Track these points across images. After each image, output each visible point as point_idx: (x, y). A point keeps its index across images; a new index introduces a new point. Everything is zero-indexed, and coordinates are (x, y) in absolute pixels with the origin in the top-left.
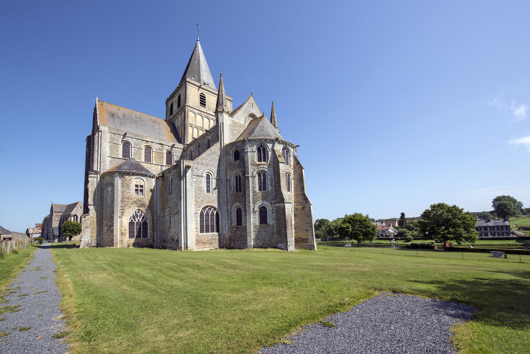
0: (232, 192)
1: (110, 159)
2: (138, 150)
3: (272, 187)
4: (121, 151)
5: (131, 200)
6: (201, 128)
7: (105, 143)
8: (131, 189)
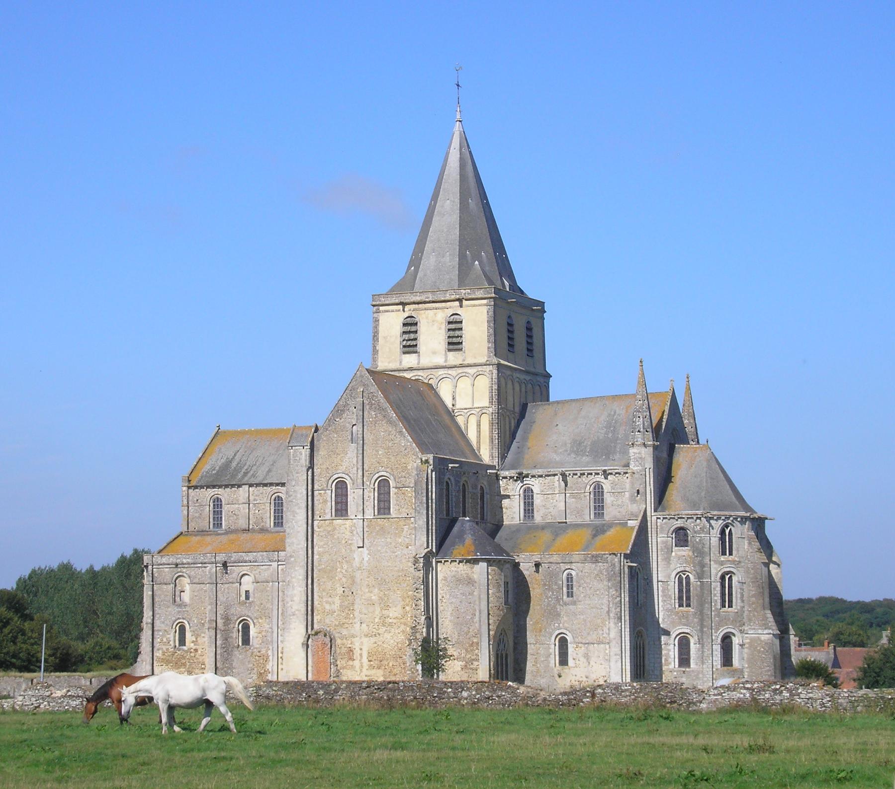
0: (671, 605)
3: (743, 601)
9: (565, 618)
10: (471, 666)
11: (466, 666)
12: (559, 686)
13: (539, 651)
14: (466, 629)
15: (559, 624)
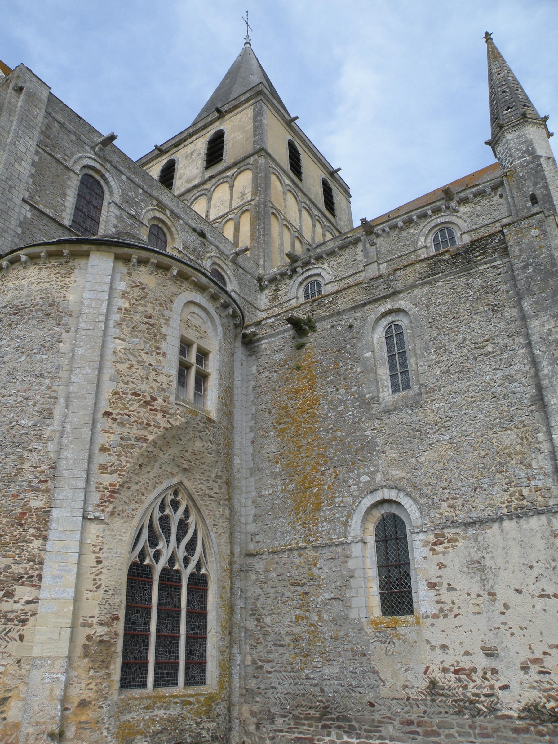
1: (29, 215)
2: (130, 221)
4: (71, 200)
5: (160, 415)
6: (298, 232)
7: (27, 139)
8: (165, 354)
9: (391, 454)
12: (384, 691)
13: (315, 571)
15: (371, 474)
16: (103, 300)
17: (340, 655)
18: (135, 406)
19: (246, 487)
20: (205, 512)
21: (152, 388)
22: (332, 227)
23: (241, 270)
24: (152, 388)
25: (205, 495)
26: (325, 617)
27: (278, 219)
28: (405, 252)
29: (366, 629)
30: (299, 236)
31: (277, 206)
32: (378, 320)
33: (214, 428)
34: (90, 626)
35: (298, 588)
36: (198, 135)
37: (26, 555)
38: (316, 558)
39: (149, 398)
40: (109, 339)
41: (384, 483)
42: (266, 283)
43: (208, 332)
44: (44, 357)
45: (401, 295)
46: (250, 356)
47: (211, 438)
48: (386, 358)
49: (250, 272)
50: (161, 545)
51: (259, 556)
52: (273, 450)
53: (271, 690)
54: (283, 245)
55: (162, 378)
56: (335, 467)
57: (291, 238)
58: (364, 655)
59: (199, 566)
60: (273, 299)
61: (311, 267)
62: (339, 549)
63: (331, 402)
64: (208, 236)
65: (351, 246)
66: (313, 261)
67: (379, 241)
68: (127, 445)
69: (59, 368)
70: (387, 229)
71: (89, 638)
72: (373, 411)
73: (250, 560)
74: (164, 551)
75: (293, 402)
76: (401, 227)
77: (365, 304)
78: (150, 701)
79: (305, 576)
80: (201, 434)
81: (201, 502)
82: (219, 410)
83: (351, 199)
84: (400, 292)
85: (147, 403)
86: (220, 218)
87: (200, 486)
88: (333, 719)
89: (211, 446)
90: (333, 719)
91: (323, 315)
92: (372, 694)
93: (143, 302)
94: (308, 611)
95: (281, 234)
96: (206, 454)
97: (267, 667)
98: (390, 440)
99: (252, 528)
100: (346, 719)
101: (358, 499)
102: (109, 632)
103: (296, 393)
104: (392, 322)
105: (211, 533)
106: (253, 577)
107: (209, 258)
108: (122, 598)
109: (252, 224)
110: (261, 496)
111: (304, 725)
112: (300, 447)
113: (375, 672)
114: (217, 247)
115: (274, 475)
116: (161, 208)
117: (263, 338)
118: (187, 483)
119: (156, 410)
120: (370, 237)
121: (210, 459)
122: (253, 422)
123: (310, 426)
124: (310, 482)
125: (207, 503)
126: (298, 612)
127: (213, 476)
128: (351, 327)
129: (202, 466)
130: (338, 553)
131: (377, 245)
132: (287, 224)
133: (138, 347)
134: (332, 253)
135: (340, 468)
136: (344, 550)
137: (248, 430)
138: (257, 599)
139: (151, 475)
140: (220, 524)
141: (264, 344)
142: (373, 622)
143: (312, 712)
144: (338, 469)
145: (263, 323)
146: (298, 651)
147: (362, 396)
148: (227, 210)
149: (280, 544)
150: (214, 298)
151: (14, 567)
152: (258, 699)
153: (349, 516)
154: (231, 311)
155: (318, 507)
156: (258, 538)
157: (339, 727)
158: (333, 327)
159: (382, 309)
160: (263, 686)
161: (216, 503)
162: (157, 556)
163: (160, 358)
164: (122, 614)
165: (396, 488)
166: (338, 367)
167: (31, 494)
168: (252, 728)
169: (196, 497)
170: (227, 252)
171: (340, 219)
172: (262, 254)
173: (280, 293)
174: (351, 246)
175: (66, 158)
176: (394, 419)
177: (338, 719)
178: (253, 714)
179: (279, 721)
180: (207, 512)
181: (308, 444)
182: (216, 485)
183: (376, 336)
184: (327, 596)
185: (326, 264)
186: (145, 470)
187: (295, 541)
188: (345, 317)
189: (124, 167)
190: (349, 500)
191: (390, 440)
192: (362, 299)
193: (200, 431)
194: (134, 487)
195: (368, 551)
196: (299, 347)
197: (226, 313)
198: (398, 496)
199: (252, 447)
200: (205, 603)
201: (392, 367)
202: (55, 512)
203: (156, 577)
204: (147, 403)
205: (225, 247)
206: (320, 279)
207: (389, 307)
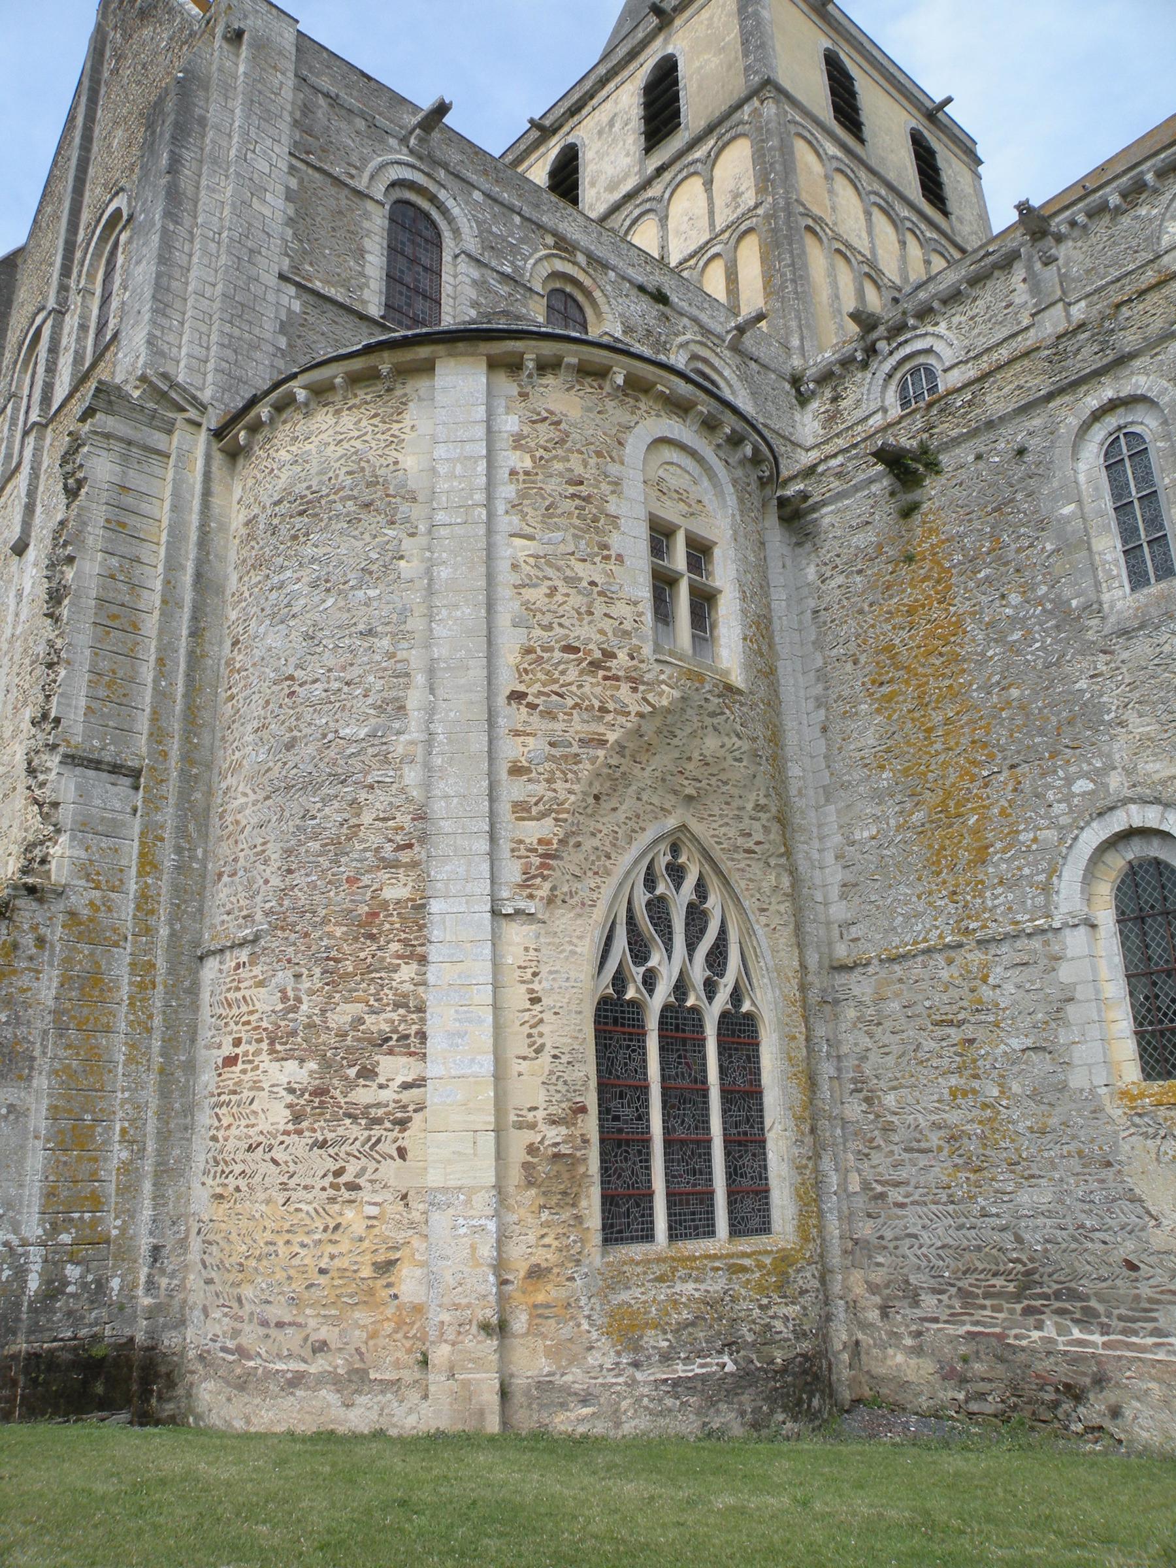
1: (297, 306)
2: (503, 290)
4: (375, 262)
5: (625, 688)
7: (269, 142)
8: (620, 558)
9: (1141, 726)
10: (364, 1095)
11: (320, 1092)
13: (986, 992)
14: (333, 814)
15: (1097, 776)
16: (475, 459)
17: (1054, 1166)
18: (572, 674)
19: (820, 826)
20: (740, 884)
21: (602, 632)
22: (944, 241)
23: (753, 365)
24: (602, 632)
25: (736, 848)
26: (1016, 1088)
27: (820, 240)
28: (1131, 267)
29: (1109, 1109)
30: (872, 274)
31: (816, 211)
32: (1085, 427)
33: (742, 705)
34: (532, 1126)
35: (952, 1031)
36: (618, 79)
37: (389, 996)
38: (985, 966)
39: (598, 654)
40: (500, 539)
41: (1129, 793)
42: (811, 386)
43: (706, 501)
44: (372, 593)
45: (1137, 363)
46: (799, 544)
47: (738, 727)
48: (1112, 513)
49: (773, 366)
50: (656, 959)
51: (860, 970)
52: (871, 742)
53: (908, 1242)
54: (837, 297)
55: (620, 609)
56: (1012, 767)
57: (854, 279)
58: (1109, 1164)
59: (736, 997)
60: (831, 418)
61: (908, 335)
62: (1036, 943)
63: (990, 625)
64: (674, 298)
65: (996, 273)
66: (911, 322)
67: (1063, 251)
68: (565, 757)
69: (404, 613)
70: (1081, 218)
71: (532, 1149)
72: (1091, 635)
73: (841, 979)
74: (663, 970)
75: (904, 634)
76: (1117, 207)
77: (1050, 397)
78: (665, 1267)
79: (965, 1004)
80: (715, 721)
81: (730, 864)
82: (748, 666)
83: (981, 169)
84: (1132, 356)
85: (595, 665)
86: (691, 256)
87: (723, 830)
88: (1046, 1297)
89: (739, 743)
90: (1046, 1297)
91: (953, 433)
92: (1130, 1245)
93: (560, 452)
94: (976, 1076)
95: (832, 274)
96: (730, 761)
97: (895, 1195)
98: (1136, 695)
99: (839, 911)
100: (1074, 1295)
101: (1069, 833)
102: (569, 1139)
103: (910, 613)
104: (1120, 428)
105: (756, 927)
106: (851, 1014)
107: (681, 346)
108: (588, 1069)
109: (764, 260)
110: (853, 844)
111: (984, 1307)
112: (929, 730)
113: (1135, 1200)
114: (695, 320)
115: (878, 796)
116: (566, 250)
117: (824, 503)
118: (696, 827)
119: (617, 678)
120: (1039, 245)
121: (740, 771)
122: (820, 686)
123: (947, 682)
124: (959, 804)
125: (742, 865)
126: (954, 1081)
127: (750, 806)
128: (1021, 452)
129: (724, 789)
130: (1035, 952)
131: (1061, 262)
132: (843, 248)
133: (562, 548)
134: (953, 298)
135: (1025, 768)
136: (1046, 943)
137: (811, 705)
138: (864, 1058)
139: (621, 816)
140: (773, 908)
141: (827, 516)
142: (1124, 1094)
143: (999, 1282)
144: (1019, 770)
145: (820, 469)
146: (960, 1161)
147: (1061, 605)
148: (706, 237)
149: (901, 942)
150: (709, 425)
151: (370, 1020)
152: (880, 1259)
153: (1053, 871)
154: (748, 450)
155: (981, 856)
156: (854, 931)
157: (1061, 1312)
158: (979, 457)
159: (1092, 401)
160: (889, 1234)
161: (761, 864)
162: (650, 981)
163: (612, 566)
164: (591, 1100)
165: (1157, 801)
166: (998, 546)
167: (383, 875)
168: (873, 1315)
169: (717, 853)
170: (719, 329)
171: (960, 220)
172: (793, 324)
173: (843, 404)
174: (996, 273)
175: (353, 172)
176: (1142, 647)
177: (1057, 1295)
178: (873, 1288)
179: (929, 1302)
180: (743, 884)
181: (948, 721)
182: (757, 825)
183: (1082, 466)
184: (1016, 1043)
185: (943, 325)
186: (606, 806)
187: (935, 933)
188: (1006, 431)
189: (476, 172)
190: (1051, 835)
191: (1136, 695)
192: (1041, 384)
193: (713, 715)
194: (589, 844)
195: (1101, 943)
196: (907, 512)
197: (739, 455)
198: (1163, 818)
199: (823, 741)
200: (757, 1072)
201: (1128, 532)
202: (435, 906)
203: (652, 1024)
204: (595, 665)
205: (713, 317)
206: (932, 360)
207: (1109, 393)
